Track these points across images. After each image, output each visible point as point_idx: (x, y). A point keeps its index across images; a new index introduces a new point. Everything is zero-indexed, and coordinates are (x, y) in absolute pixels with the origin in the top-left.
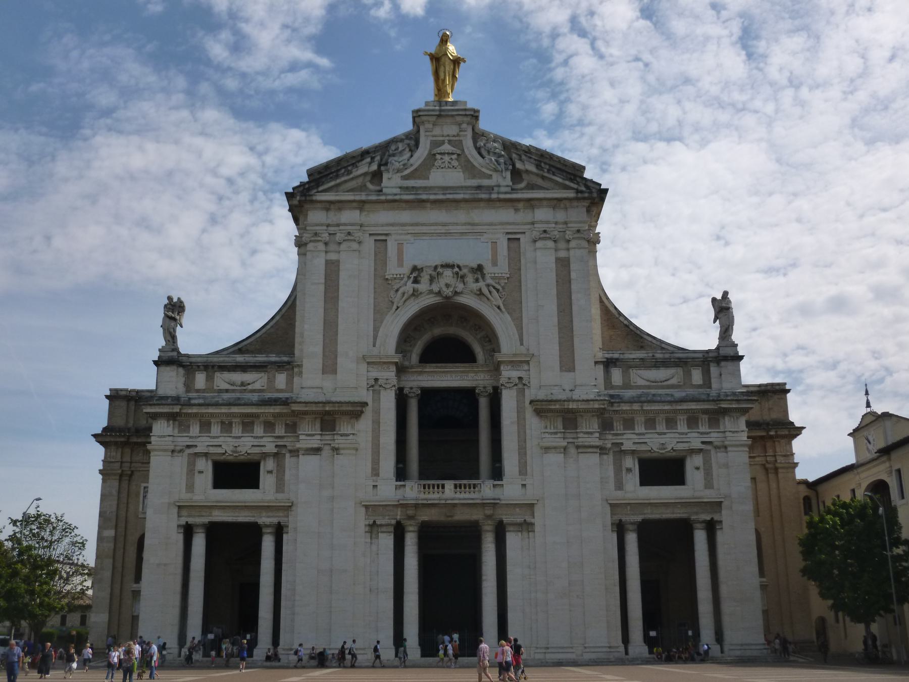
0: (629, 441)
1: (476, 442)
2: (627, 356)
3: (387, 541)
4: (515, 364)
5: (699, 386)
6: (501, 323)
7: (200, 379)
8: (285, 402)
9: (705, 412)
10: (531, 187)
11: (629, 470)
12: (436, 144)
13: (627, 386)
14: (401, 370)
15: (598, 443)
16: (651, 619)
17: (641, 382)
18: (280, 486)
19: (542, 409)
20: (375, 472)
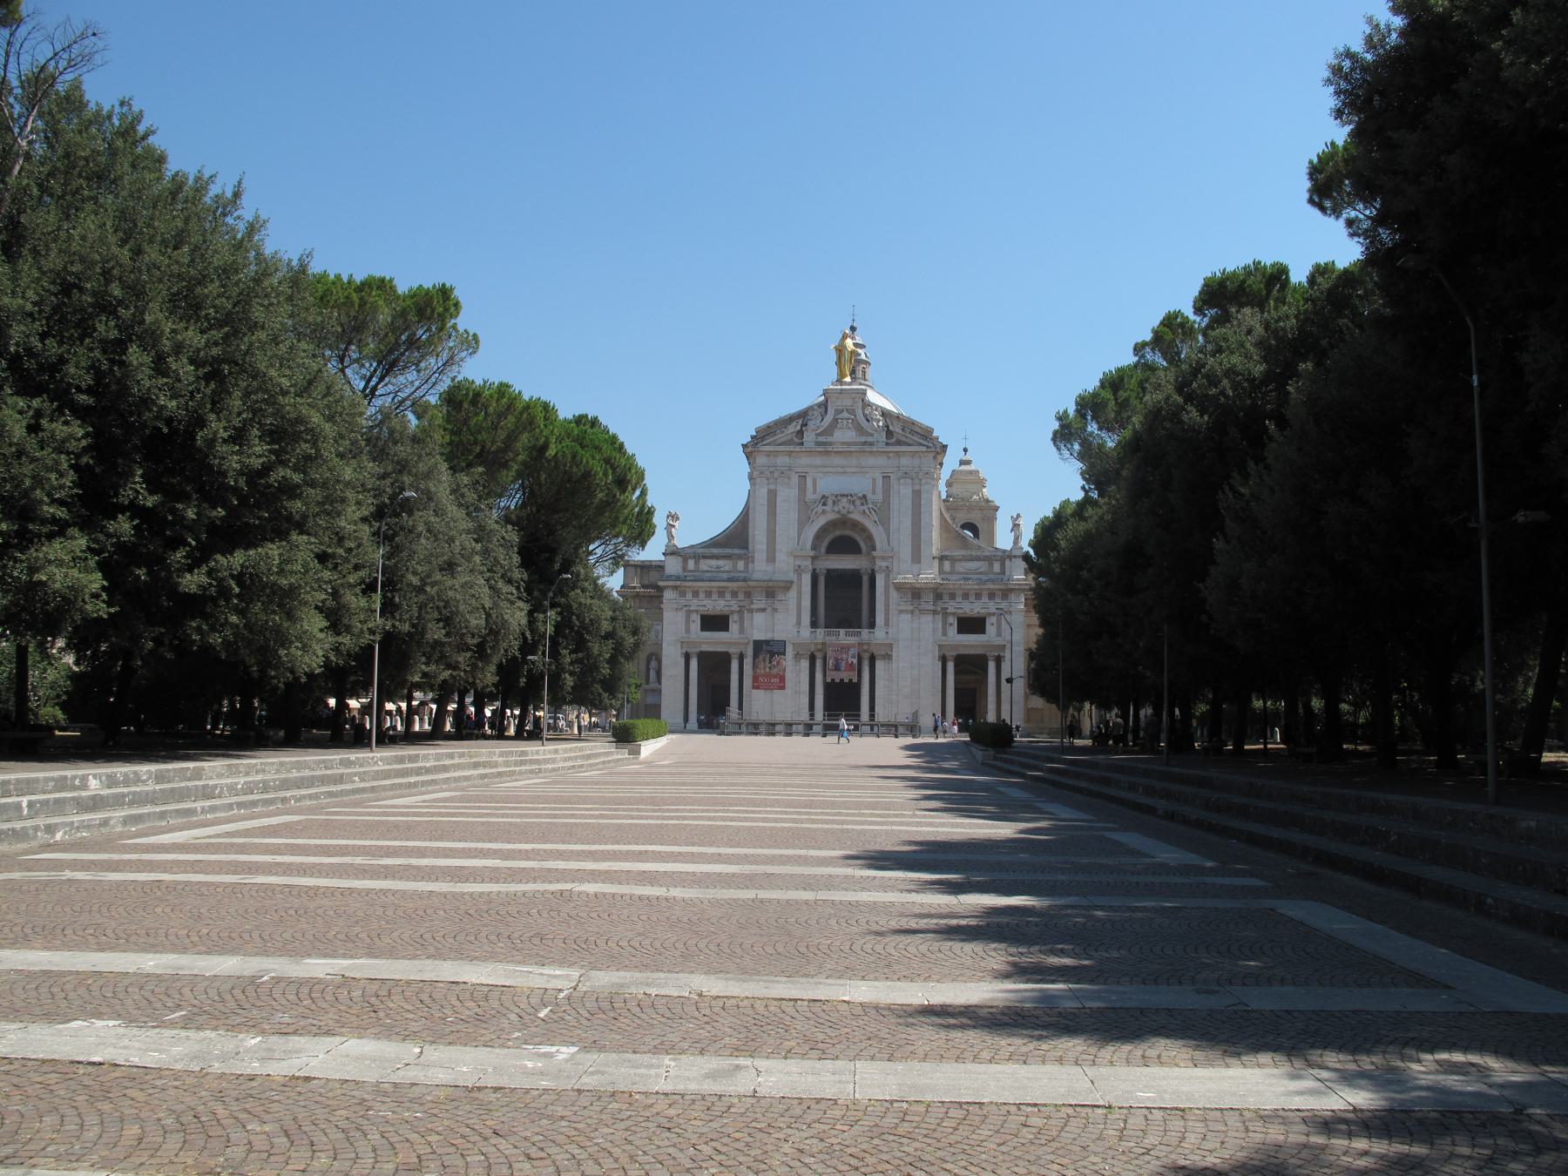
0: (952, 607)
1: (860, 599)
2: (954, 554)
3: (805, 664)
4: (884, 558)
5: (998, 574)
6: (877, 532)
7: (691, 564)
8: (745, 580)
9: (1000, 590)
10: (899, 443)
11: (951, 624)
12: (839, 412)
13: (951, 573)
14: (814, 558)
15: (932, 608)
16: (958, 713)
17: (961, 570)
18: (742, 630)
19: (900, 588)
20: (799, 623)
